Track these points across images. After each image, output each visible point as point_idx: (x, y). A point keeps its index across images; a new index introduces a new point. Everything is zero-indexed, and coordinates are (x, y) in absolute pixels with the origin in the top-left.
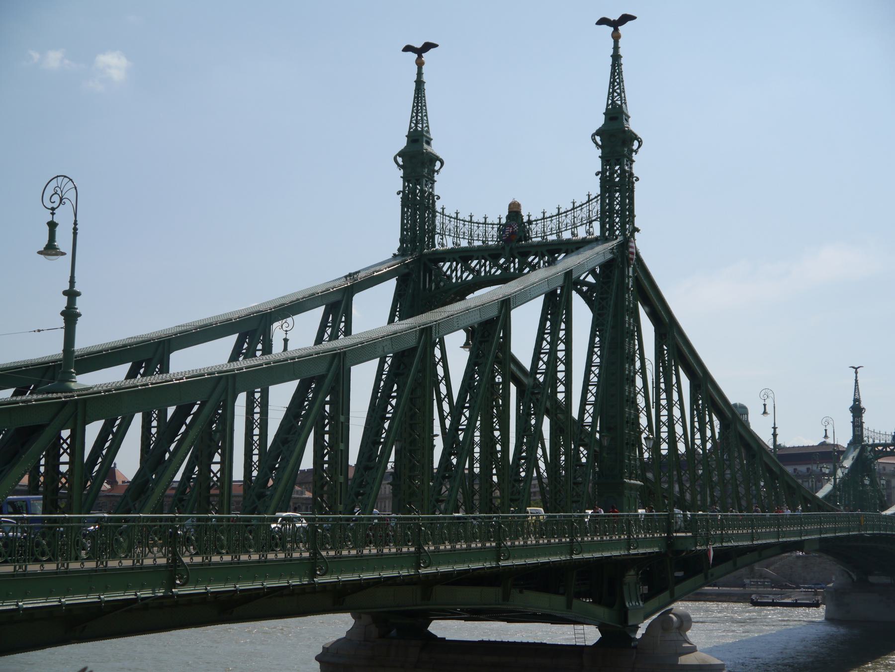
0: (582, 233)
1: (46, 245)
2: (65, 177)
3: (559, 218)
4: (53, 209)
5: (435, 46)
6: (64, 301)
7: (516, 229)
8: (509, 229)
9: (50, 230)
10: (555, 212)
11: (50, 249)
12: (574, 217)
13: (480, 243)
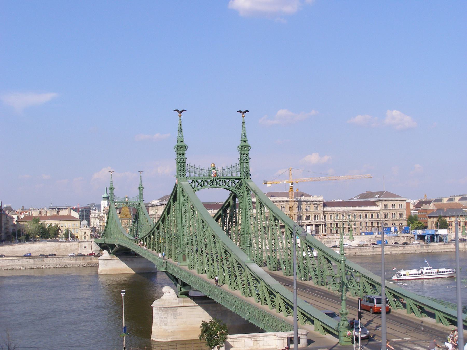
0: (234, 174)
5: (185, 111)
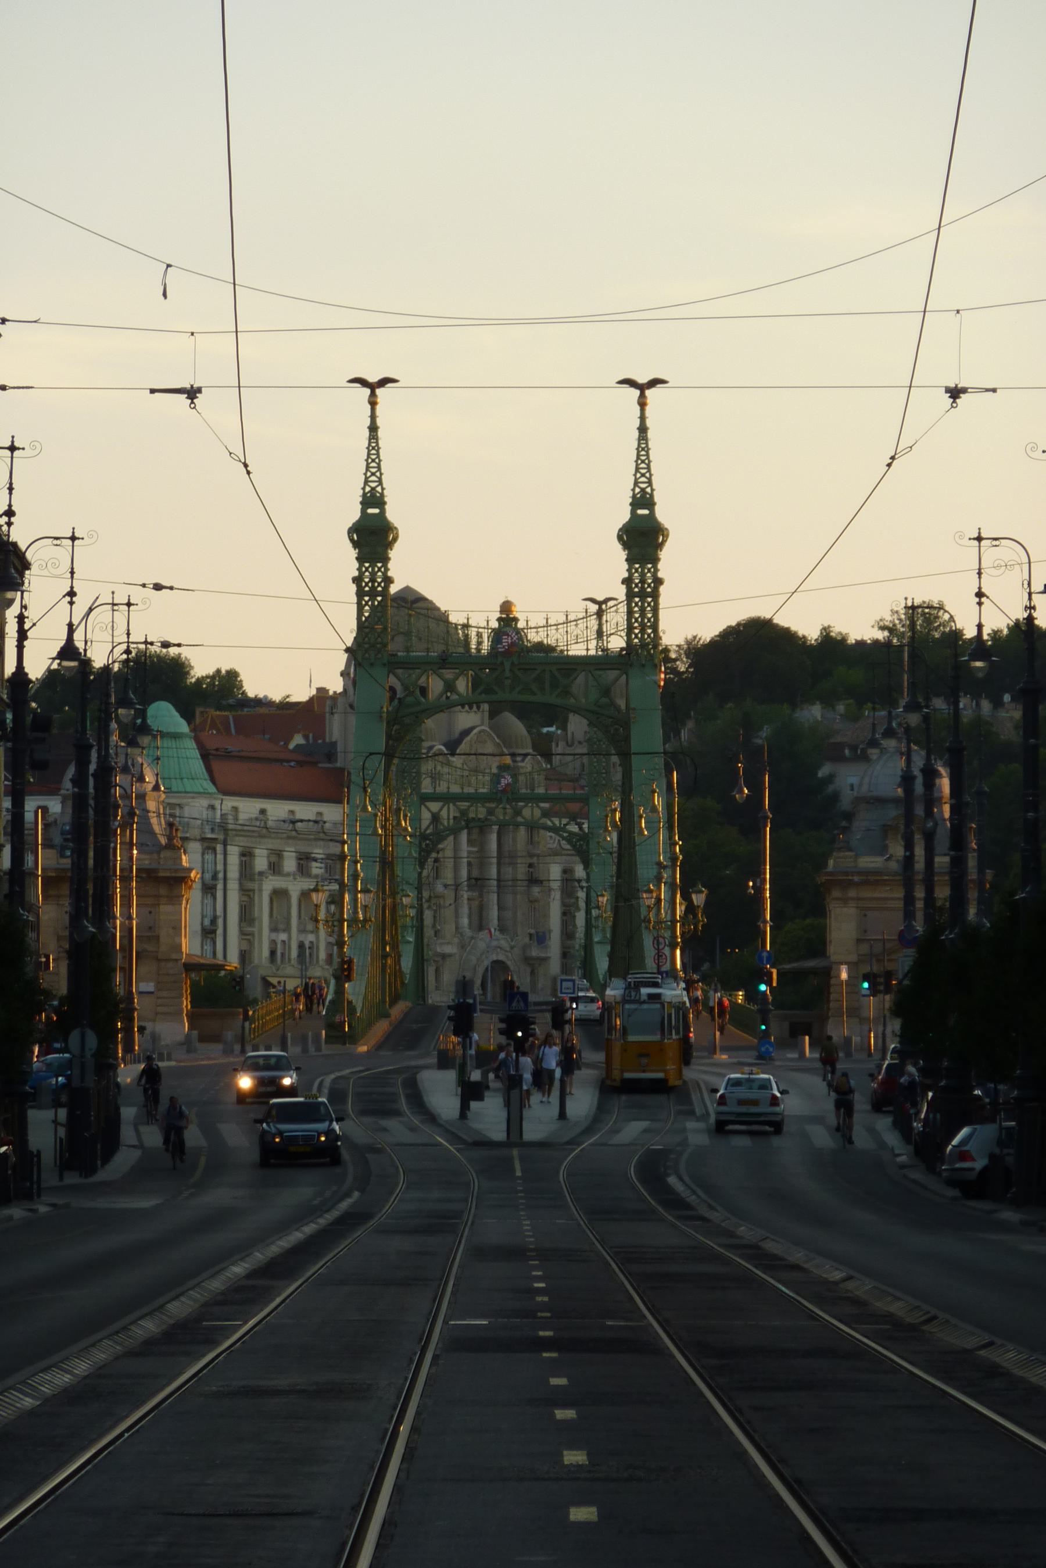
3: (567, 627)
7: (515, 639)
8: (507, 639)
10: (563, 619)
12: (587, 627)
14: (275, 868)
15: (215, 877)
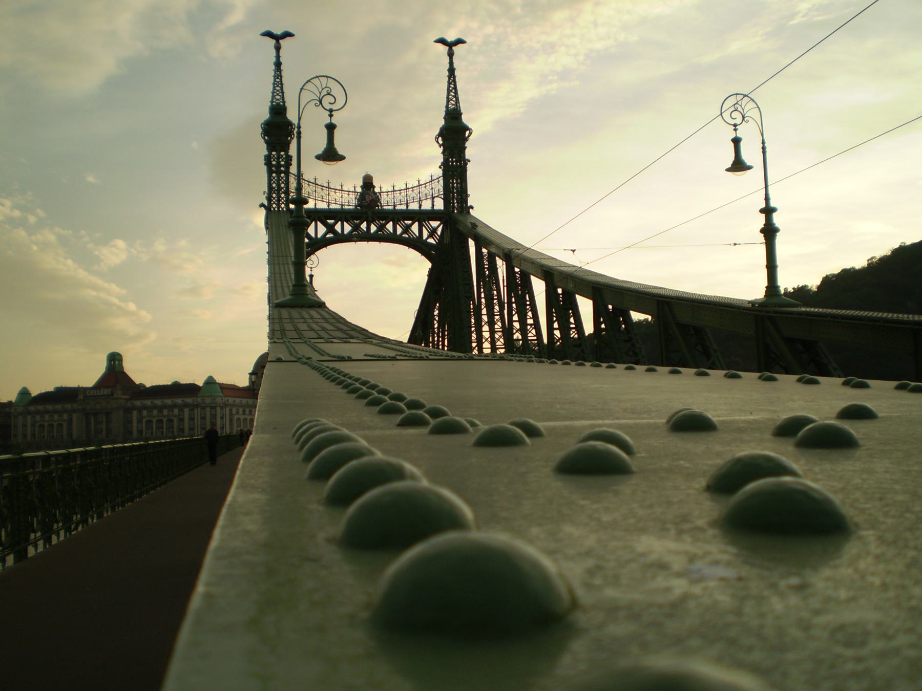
0: (427, 205)
1: (733, 162)
2: (737, 94)
4: (735, 125)
6: (761, 220)
8: (369, 197)
9: (734, 146)
10: (404, 187)
11: (739, 165)
13: (338, 207)
14: (237, 413)
15: (223, 415)
